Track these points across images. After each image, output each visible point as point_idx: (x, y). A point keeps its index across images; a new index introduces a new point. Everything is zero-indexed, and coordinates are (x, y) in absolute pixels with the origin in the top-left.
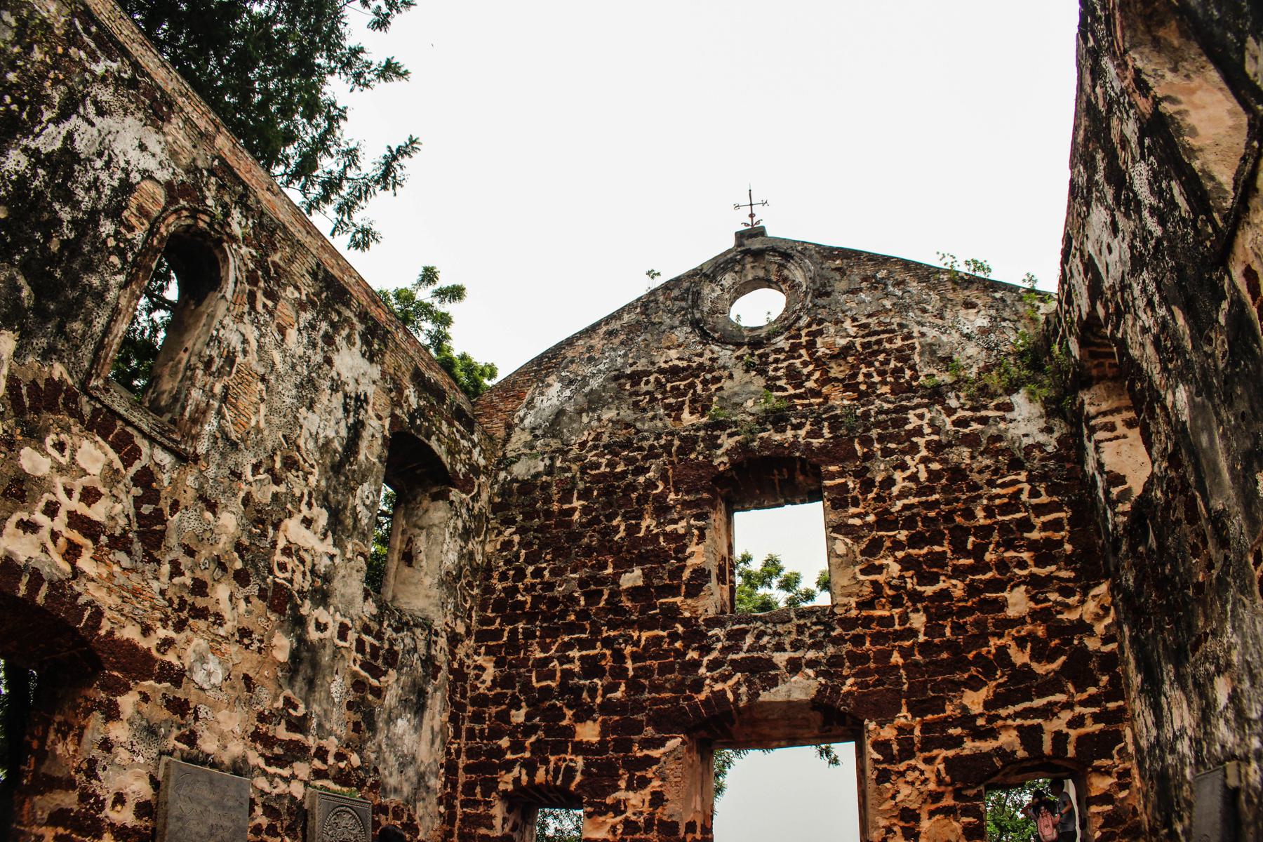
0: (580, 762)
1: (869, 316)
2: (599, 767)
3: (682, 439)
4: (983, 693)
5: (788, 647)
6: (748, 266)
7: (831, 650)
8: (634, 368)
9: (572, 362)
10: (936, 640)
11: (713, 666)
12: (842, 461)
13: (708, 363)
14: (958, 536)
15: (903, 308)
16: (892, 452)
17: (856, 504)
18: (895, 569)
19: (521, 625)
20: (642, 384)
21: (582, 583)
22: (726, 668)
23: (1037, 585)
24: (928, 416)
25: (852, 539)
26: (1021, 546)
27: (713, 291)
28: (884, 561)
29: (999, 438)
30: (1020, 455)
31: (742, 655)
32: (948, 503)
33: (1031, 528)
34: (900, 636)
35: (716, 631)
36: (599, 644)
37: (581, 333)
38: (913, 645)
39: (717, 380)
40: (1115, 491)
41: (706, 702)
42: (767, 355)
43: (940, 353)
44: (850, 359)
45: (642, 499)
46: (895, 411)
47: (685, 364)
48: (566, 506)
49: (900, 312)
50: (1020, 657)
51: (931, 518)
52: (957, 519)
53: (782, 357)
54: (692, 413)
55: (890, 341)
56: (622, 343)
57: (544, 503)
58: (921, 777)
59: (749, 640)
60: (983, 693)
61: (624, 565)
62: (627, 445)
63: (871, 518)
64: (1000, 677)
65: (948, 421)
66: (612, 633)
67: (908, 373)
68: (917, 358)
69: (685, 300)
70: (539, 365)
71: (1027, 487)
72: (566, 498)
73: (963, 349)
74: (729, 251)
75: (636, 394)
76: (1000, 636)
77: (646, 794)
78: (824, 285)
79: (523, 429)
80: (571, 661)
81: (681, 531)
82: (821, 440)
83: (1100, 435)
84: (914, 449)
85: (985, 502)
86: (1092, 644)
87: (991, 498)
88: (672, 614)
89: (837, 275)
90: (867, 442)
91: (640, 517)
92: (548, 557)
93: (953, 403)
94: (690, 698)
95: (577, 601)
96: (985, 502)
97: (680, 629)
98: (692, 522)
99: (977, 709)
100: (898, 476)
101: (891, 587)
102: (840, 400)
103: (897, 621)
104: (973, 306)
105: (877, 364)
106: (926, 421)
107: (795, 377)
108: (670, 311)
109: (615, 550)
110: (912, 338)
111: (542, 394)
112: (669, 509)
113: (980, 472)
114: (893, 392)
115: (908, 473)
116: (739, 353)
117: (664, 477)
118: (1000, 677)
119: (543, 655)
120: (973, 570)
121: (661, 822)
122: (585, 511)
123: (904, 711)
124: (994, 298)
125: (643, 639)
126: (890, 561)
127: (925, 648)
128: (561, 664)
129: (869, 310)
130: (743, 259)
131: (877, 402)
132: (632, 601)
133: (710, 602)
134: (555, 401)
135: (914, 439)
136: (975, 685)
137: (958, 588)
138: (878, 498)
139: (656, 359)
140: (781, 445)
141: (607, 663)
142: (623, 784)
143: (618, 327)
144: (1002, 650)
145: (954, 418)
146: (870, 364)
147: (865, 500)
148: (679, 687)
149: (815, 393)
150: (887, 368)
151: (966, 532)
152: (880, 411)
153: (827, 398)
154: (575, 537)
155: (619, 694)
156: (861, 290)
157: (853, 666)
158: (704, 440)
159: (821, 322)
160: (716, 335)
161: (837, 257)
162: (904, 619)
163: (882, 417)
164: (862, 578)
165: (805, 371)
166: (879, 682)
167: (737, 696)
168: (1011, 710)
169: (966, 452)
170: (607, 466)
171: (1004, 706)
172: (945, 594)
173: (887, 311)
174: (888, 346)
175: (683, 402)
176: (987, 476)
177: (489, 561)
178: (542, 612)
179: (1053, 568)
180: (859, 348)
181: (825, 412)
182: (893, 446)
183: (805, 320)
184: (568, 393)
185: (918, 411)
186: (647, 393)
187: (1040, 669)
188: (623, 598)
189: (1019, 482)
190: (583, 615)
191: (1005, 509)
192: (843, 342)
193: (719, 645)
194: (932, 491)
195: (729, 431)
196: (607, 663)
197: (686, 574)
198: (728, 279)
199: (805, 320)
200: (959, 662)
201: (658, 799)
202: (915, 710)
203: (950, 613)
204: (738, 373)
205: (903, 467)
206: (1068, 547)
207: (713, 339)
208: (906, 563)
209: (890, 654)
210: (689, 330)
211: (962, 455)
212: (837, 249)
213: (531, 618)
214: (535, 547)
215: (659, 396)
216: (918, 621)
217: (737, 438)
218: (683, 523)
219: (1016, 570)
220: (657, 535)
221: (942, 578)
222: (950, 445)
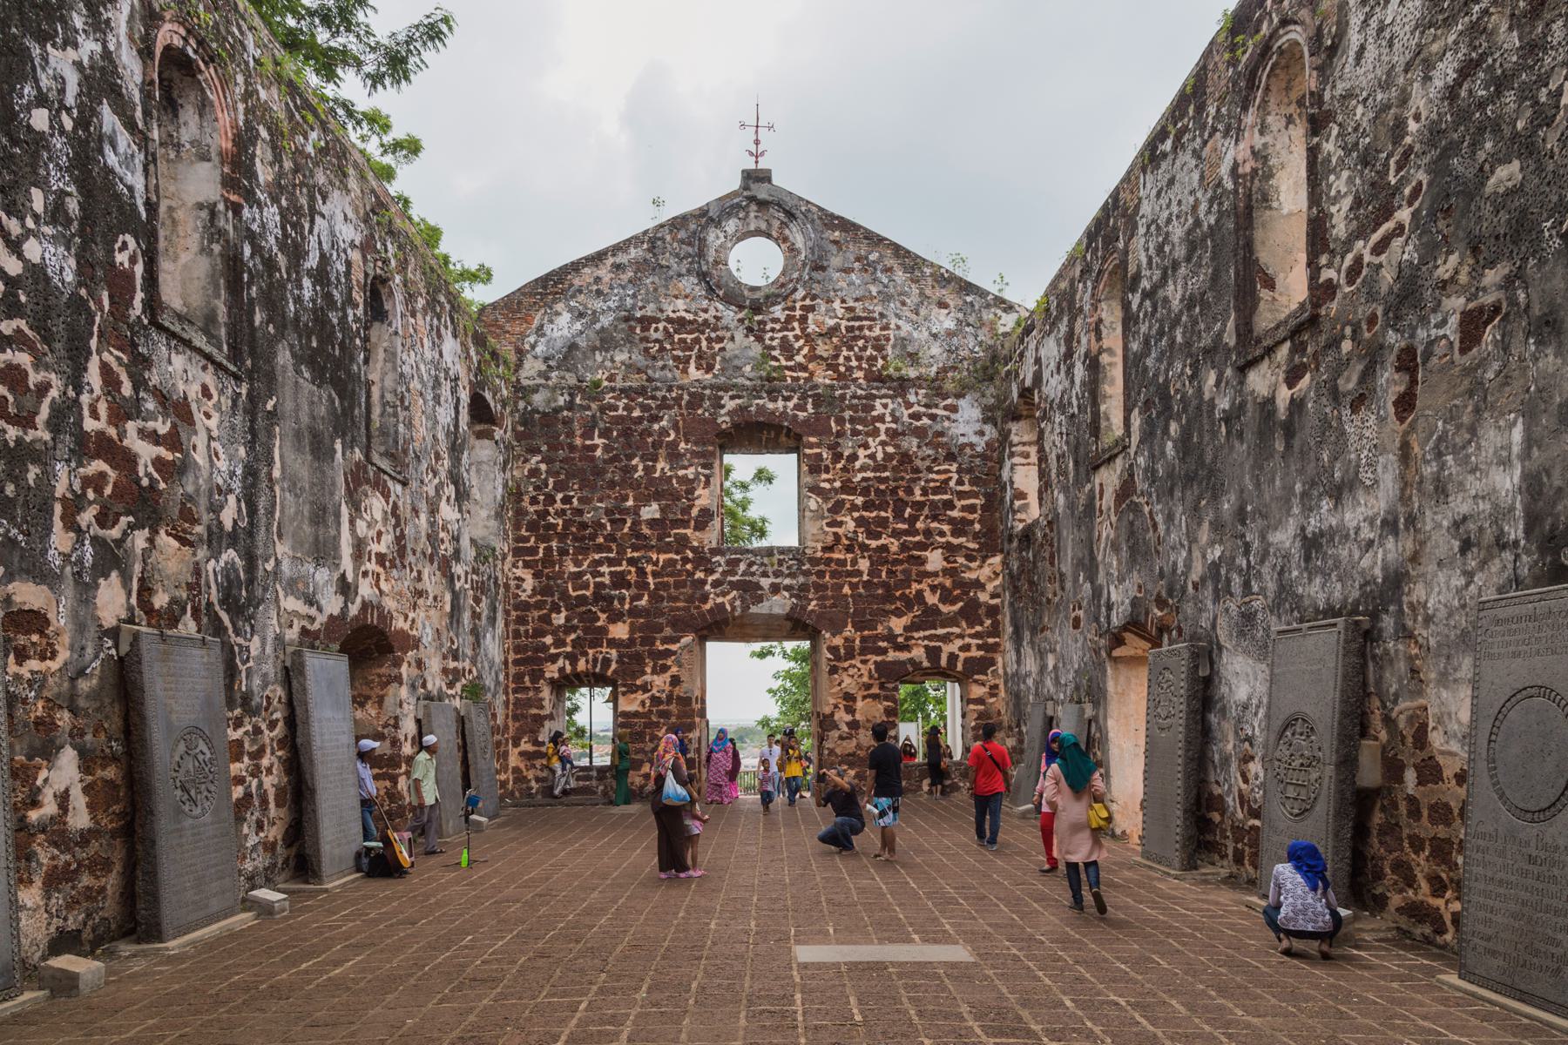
0: (614, 653)
1: (857, 300)
2: (630, 657)
3: (690, 394)
4: (905, 620)
6: (752, 215)
7: (801, 579)
9: (580, 292)
11: (716, 584)
13: (713, 321)
15: (886, 298)
17: (827, 470)
18: (851, 525)
19: (554, 544)
21: (608, 512)
22: (725, 587)
23: (950, 550)
24: (891, 406)
29: (941, 434)
32: (895, 480)
33: (953, 507)
34: (850, 574)
37: (586, 258)
39: (720, 340)
40: (1017, 503)
41: (711, 611)
43: (910, 349)
44: (835, 340)
45: (657, 445)
46: (866, 397)
50: (932, 599)
52: (901, 493)
53: (778, 326)
55: (870, 328)
58: (859, 671)
59: (742, 567)
60: (905, 620)
61: (644, 500)
62: (642, 391)
64: (917, 611)
67: (880, 362)
68: (889, 350)
69: (687, 239)
70: (545, 287)
71: (956, 476)
72: (588, 434)
74: (734, 194)
76: (920, 582)
77: (667, 677)
78: (821, 258)
79: (536, 357)
80: (602, 575)
83: (1017, 460)
84: (875, 433)
86: (983, 597)
87: (927, 481)
88: (683, 542)
89: (834, 248)
90: (840, 421)
91: (655, 460)
93: (912, 398)
94: (698, 608)
95: (603, 526)
97: (690, 555)
99: (898, 631)
100: (861, 453)
102: (823, 378)
108: (677, 255)
109: (635, 486)
111: (551, 322)
112: (679, 456)
114: (865, 378)
117: (676, 427)
118: (917, 611)
121: (679, 698)
122: (607, 448)
123: (849, 627)
126: (848, 519)
127: (867, 585)
129: (858, 293)
134: (565, 332)
136: (898, 613)
138: (844, 469)
139: (665, 307)
140: (773, 413)
141: (632, 578)
142: (648, 670)
144: (920, 593)
146: (850, 348)
148: (690, 599)
151: (906, 504)
152: (854, 396)
153: (812, 374)
155: (644, 602)
157: (816, 592)
159: (814, 298)
161: (833, 228)
162: (854, 562)
165: (797, 345)
166: (833, 605)
167: (733, 608)
168: (922, 634)
169: (915, 441)
171: (917, 630)
172: (884, 548)
174: (867, 332)
176: (927, 463)
177: (519, 486)
181: (811, 388)
182: (860, 427)
183: (801, 293)
184: (578, 326)
186: (657, 341)
187: (945, 609)
190: (611, 538)
191: (936, 491)
192: (831, 322)
194: (885, 469)
196: (632, 578)
197: (695, 512)
198: (731, 225)
199: (801, 293)
200: (888, 597)
201: (676, 680)
202: (858, 627)
203: (887, 562)
204: (739, 336)
205: (866, 446)
206: (977, 527)
208: (860, 522)
209: (842, 587)
211: (910, 444)
212: (838, 218)
213: (562, 537)
216: (864, 565)
218: (692, 470)
222: (903, 434)
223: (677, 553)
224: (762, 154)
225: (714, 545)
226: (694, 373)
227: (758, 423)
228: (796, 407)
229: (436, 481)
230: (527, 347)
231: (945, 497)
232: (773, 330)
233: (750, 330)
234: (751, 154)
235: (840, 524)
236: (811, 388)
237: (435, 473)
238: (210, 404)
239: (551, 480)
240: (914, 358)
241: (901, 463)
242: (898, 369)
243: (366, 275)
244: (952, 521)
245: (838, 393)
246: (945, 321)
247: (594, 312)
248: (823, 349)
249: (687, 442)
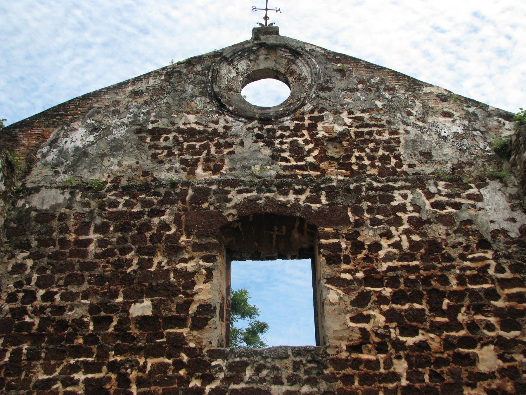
1: (363, 111)
3: (195, 190)
5: (285, 380)
6: (262, 57)
8: (155, 125)
9: (98, 113)
10: (417, 385)
12: (337, 225)
13: (221, 130)
14: (435, 298)
16: (380, 222)
17: (347, 262)
20: (162, 140)
23: (504, 347)
24: (410, 197)
25: (344, 291)
26: (489, 312)
28: (372, 312)
29: (469, 222)
30: (488, 237)
31: (242, 385)
33: (497, 297)
35: (219, 362)
36: (105, 368)
37: (108, 89)
38: (397, 387)
42: (274, 131)
44: (345, 143)
46: (381, 189)
47: (201, 128)
49: (389, 112)
51: (412, 281)
52: (433, 283)
53: (287, 133)
54: (205, 170)
55: (380, 133)
56: (146, 103)
57: (61, 232)
59: (249, 373)
61: (135, 296)
62: (145, 188)
63: (360, 275)
65: (427, 203)
66: (119, 358)
67: (393, 161)
68: (401, 150)
71: (493, 263)
72: (84, 228)
73: (441, 148)
74: (247, 42)
75: (156, 147)
78: (326, 82)
82: (319, 205)
84: (398, 222)
85: (458, 272)
88: (177, 344)
89: (338, 76)
90: (357, 211)
91: (152, 253)
92: (61, 282)
93: (433, 189)
95: (86, 325)
96: (458, 272)
97: (185, 358)
98: (201, 262)
100: (384, 242)
101: (377, 335)
102: (337, 176)
103: (382, 365)
105: (367, 150)
106: (409, 200)
107: (297, 152)
110: (398, 133)
113: (454, 247)
115: (393, 241)
116: (250, 125)
117: (177, 220)
119: (46, 377)
120: (448, 327)
122: (101, 243)
125: (149, 365)
128: (65, 385)
130: (257, 50)
131: (368, 180)
132: (140, 329)
133: (212, 335)
134: (79, 144)
135: (399, 214)
137: (435, 341)
138: (367, 259)
140: (283, 205)
143: (144, 89)
145: (433, 200)
146: (362, 150)
149: (314, 167)
150: (376, 154)
151: (442, 295)
152: (371, 187)
153: (323, 172)
154: (91, 266)
156: (357, 90)
158: (215, 192)
159: (322, 110)
160: (231, 108)
161: (339, 61)
162: (388, 364)
163: (371, 193)
164: (352, 324)
165: (307, 148)
170: (125, 205)
172: (423, 346)
173: (378, 110)
174: (377, 137)
175: (198, 160)
178: (49, 334)
179: (517, 333)
180: (353, 136)
181: (324, 182)
182: (380, 217)
183: (308, 107)
184: (92, 138)
185: (402, 192)
186: (165, 148)
188: (132, 326)
190: (91, 339)
191: (474, 280)
192: (339, 129)
193: (222, 375)
194: (413, 258)
195: (238, 188)
197: (193, 308)
198: (243, 65)
199: (308, 107)
203: (428, 363)
204: (249, 142)
205: (388, 235)
207: (228, 111)
208: (390, 316)
210: (208, 100)
211: (439, 231)
214: (48, 272)
215: (177, 152)
216: (401, 367)
219: (485, 331)
220: (168, 271)
221: (421, 331)
223: (169, 357)
225: (215, 345)
227: (267, 214)
228: (308, 199)
230: (39, 156)
231: (486, 286)
235: (367, 319)
239: (35, 276)
240: (427, 156)
241: (429, 252)
242: (411, 166)
244: (498, 312)
245: (352, 187)
248: (331, 152)
249: (188, 237)
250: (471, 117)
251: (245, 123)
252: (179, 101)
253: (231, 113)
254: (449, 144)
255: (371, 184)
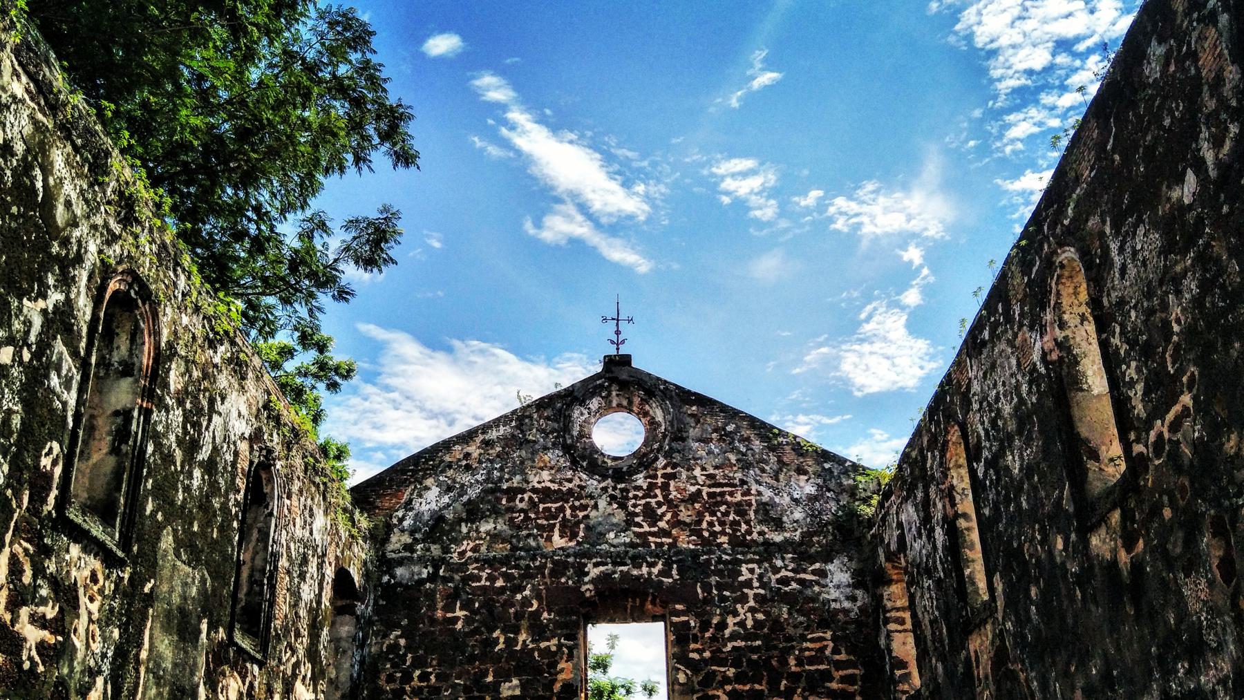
1: (716, 467)
3: (553, 562)
6: (614, 393)
9: (450, 466)
15: (746, 466)
17: (695, 641)
24: (758, 571)
27: (582, 414)
33: (831, 679)
37: (457, 437)
39: (584, 508)
40: (898, 673)
42: (628, 491)
48: (449, 615)
53: (640, 494)
54: (561, 537)
56: (498, 456)
62: (505, 561)
63: (707, 654)
67: (744, 527)
70: (416, 465)
72: (449, 607)
74: (597, 376)
79: (403, 531)
81: (554, 649)
83: (892, 626)
84: (743, 599)
89: (692, 422)
90: (707, 588)
91: (517, 632)
92: (434, 663)
93: (779, 563)
100: (731, 620)
104: (805, 473)
105: (719, 514)
108: (543, 431)
109: (496, 658)
111: (420, 496)
115: (738, 619)
117: (538, 597)
122: (468, 620)
124: (824, 468)
130: (610, 385)
134: (433, 506)
135: (746, 590)
138: (714, 639)
139: (531, 478)
145: (778, 576)
146: (713, 514)
147: (703, 637)
149: (666, 533)
152: (720, 560)
153: (676, 539)
165: (659, 512)
173: (732, 465)
174: (728, 498)
176: (800, 631)
181: (677, 554)
182: (727, 593)
185: (750, 566)
186: (522, 510)
189: (824, 639)
191: (811, 661)
192: (693, 489)
197: (557, 687)
198: (594, 403)
199: (661, 462)
205: (735, 614)
212: (695, 394)
215: (533, 516)
217: (602, 568)
218: (555, 641)
220: (533, 650)
224: (623, 342)
226: (558, 541)
228: (661, 573)
229: (294, 660)
230: (395, 521)
232: (635, 497)
233: (613, 498)
234: (612, 342)
236: (677, 554)
237: (294, 651)
238: (95, 588)
242: (761, 533)
243: (251, 463)
246: (807, 488)
247: (463, 485)
248: (685, 515)
250: (826, 475)
251: (599, 482)
252: (532, 454)
253: (585, 470)
254: (799, 509)
255: (720, 558)
